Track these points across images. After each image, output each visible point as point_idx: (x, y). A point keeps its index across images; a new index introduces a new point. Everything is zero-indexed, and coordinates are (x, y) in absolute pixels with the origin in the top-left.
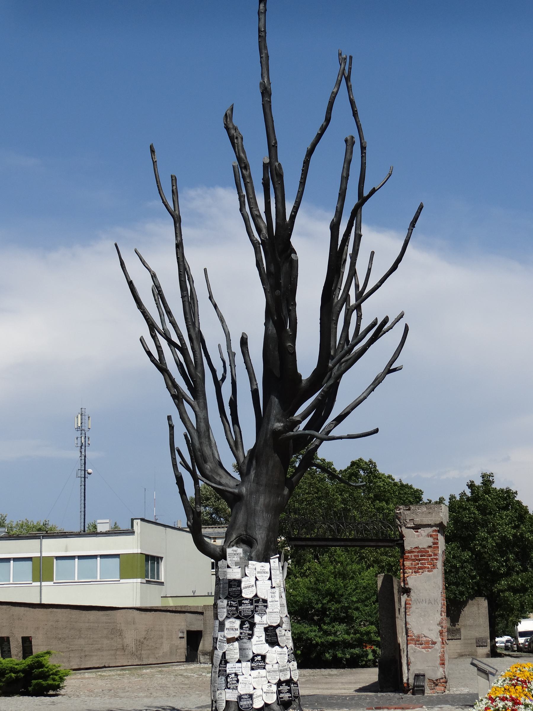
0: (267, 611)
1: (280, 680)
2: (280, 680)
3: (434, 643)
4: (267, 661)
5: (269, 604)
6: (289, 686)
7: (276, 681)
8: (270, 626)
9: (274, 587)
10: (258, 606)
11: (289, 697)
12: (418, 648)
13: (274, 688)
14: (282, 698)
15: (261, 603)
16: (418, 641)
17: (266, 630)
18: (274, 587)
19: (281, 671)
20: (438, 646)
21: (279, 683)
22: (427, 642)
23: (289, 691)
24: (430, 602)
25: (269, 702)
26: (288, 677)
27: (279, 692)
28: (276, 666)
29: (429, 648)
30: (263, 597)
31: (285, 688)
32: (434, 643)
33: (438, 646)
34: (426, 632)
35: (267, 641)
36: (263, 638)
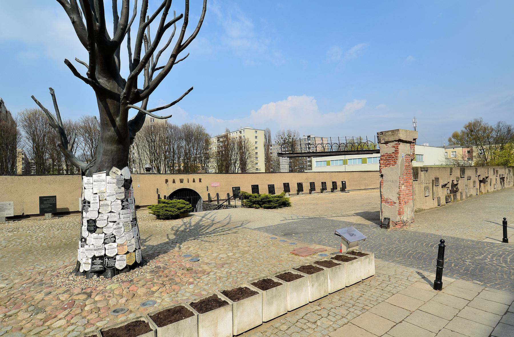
0: (89, 209)
1: (94, 256)
2: (94, 256)
3: (395, 203)
4: (87, 242)
5: (91, 205)
6: (103, 260)
7: (92, 256)
8: (91, 220)
9: (96, 194)
10: (84, 206)
11: (100, 268)
12: (387, 205)
13: (90, 261)
14: (94, 268)
15: (87, 204)
16: (386, 201)
17: (88, 221)
18: (96, 194)
19: (95, 250)
20: (397, 205)
21: (94, 258)
22: (391, 202)
23: (102, 264)
24: (393, 182)
25: (86, 270)
26: (103, 254)
27: (93, 264)
28: (91, 247)
29: (392, 205)
30: (88, 200)
31: (98, 261)
32: (395, 203)
33: (397, 205)
34: (390, 197)
35: (87, 229)
36: (86, 227)
